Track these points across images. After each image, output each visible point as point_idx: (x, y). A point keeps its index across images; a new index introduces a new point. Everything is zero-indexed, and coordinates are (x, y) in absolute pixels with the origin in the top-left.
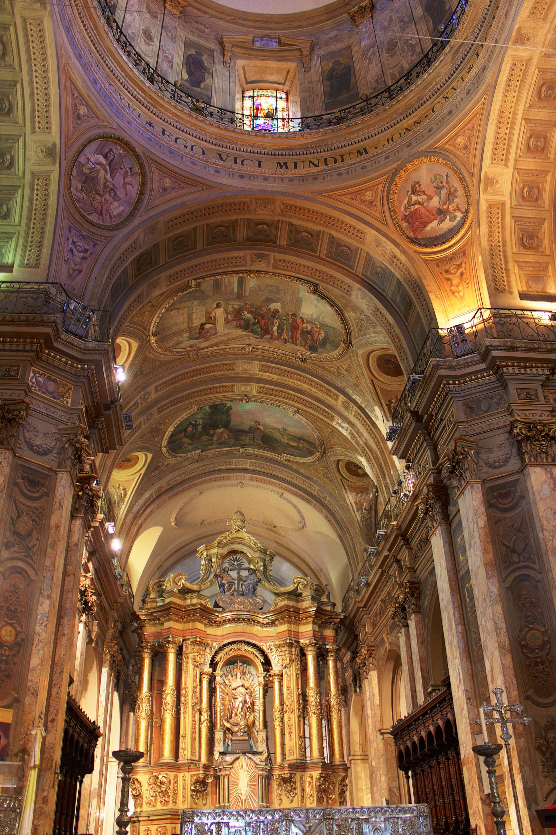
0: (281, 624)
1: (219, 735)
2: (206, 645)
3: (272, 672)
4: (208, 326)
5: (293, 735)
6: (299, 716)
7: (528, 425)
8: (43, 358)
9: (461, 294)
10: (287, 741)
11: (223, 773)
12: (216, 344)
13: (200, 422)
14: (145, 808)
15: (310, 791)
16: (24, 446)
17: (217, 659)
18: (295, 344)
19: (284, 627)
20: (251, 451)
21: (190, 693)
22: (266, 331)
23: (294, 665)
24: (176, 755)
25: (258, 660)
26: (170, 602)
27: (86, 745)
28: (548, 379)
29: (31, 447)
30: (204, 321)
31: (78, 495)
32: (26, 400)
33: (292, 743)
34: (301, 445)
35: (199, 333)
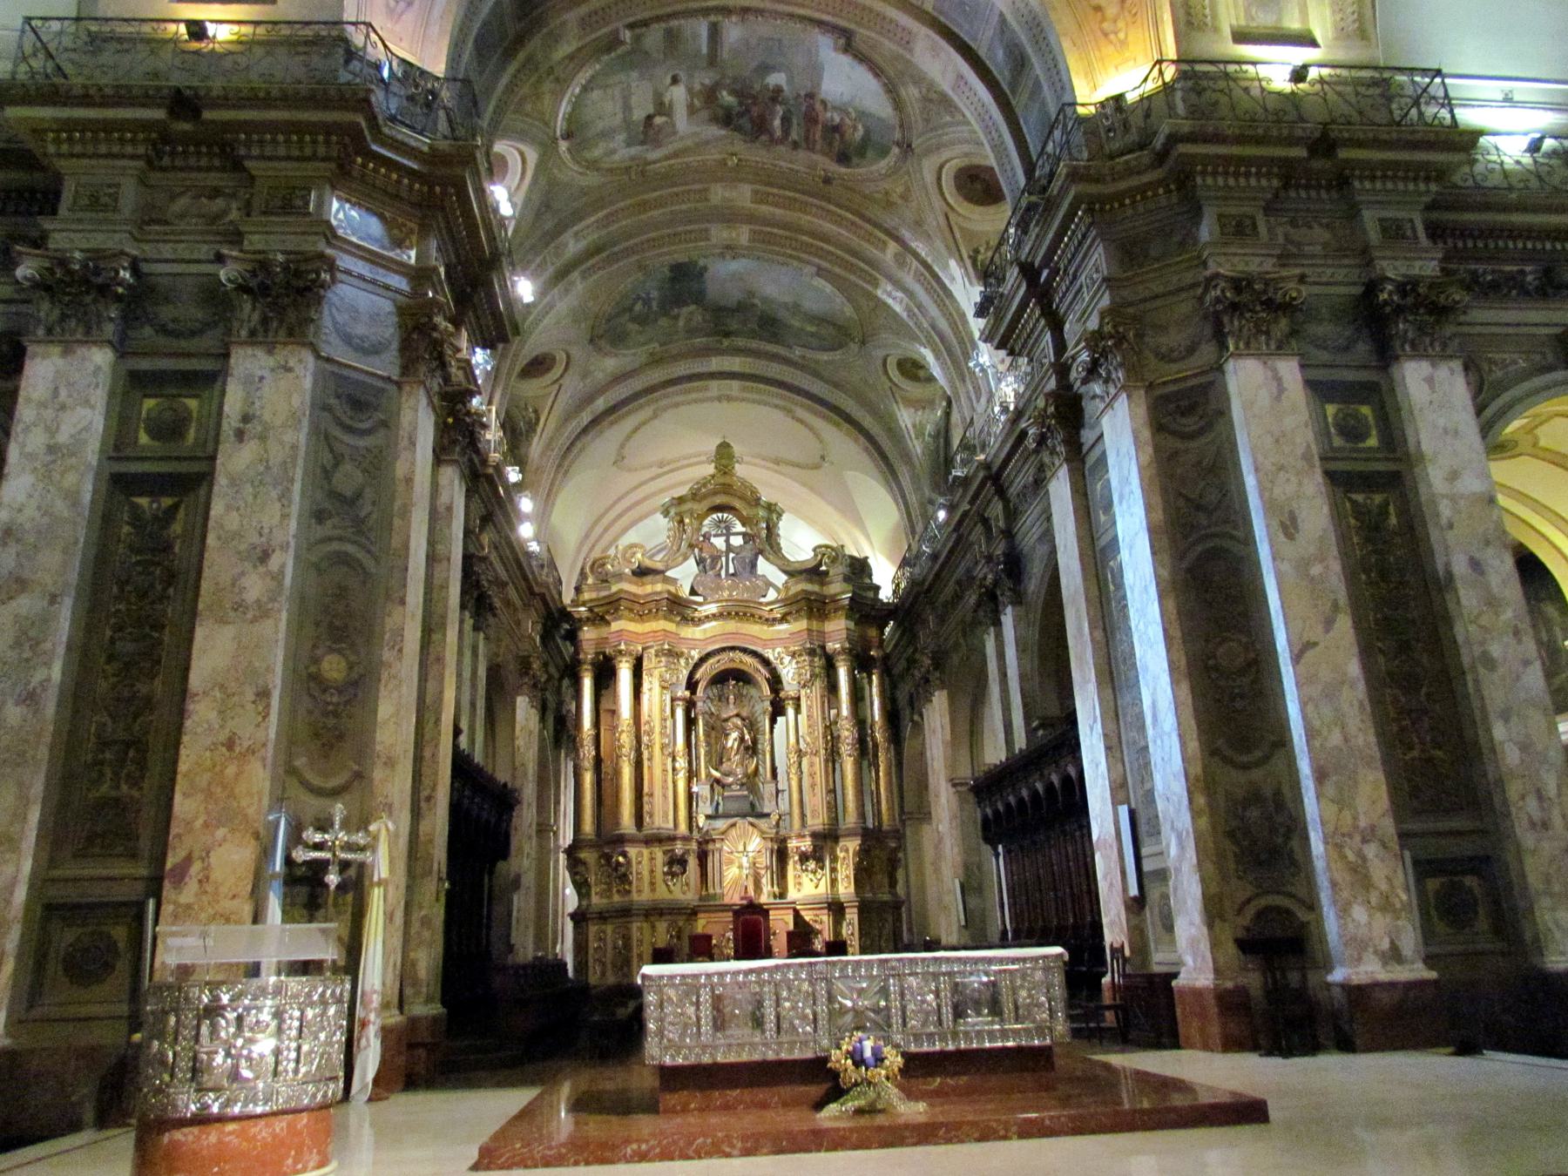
0: (796, 620)
2: (679, 655)
3: (782, 694)
4: (658, 120)
5: (818, 789)
6: (826, 761)
7: (1238, 284)
8: (355, 173)
9: (1121, 35)
10: (806, 798)
11: (710, 847)
12: (675, 155)
13: (655, 294)
14: (595, 899)
15: (846, 872)
16: (334, 339)
17: (698, 676)
18: (812, 150)
19: (803, 624)
20: (740, 342)
21: (657, 730)
22: (759, 128)
23: (818, 683)
25: (761, 675)
26: (621, 591)
27: (493, 820)
28: (1276, 196)
29: (348, 339)
30: (651, 110)
31: (445, 423)
32: (329, 251)
34: (823, 332)
35: (645, 133)
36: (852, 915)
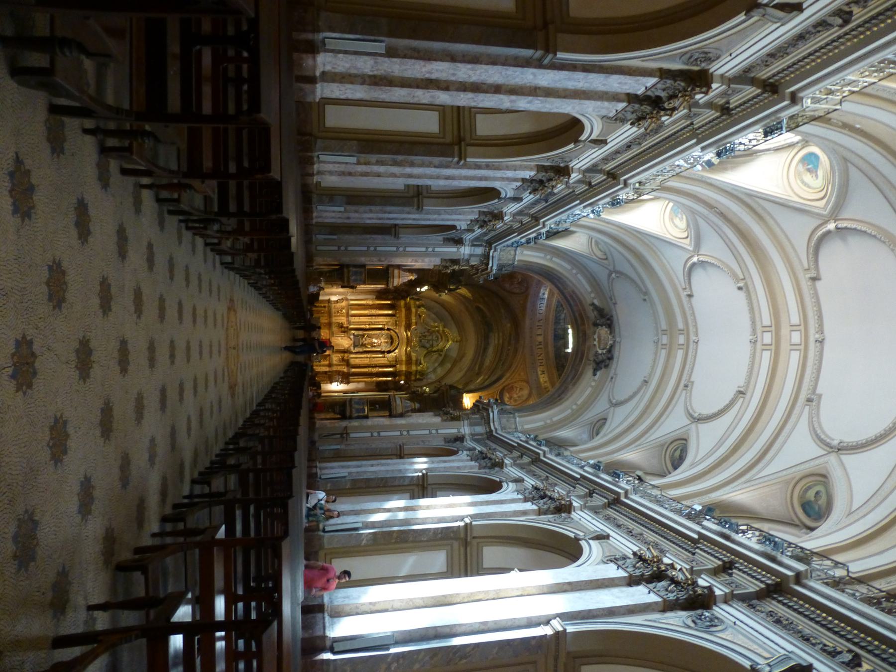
1: (361, 333)
15: (339, 368)
19: (404, 358)
33: (357, 361)
36: (327, 369)
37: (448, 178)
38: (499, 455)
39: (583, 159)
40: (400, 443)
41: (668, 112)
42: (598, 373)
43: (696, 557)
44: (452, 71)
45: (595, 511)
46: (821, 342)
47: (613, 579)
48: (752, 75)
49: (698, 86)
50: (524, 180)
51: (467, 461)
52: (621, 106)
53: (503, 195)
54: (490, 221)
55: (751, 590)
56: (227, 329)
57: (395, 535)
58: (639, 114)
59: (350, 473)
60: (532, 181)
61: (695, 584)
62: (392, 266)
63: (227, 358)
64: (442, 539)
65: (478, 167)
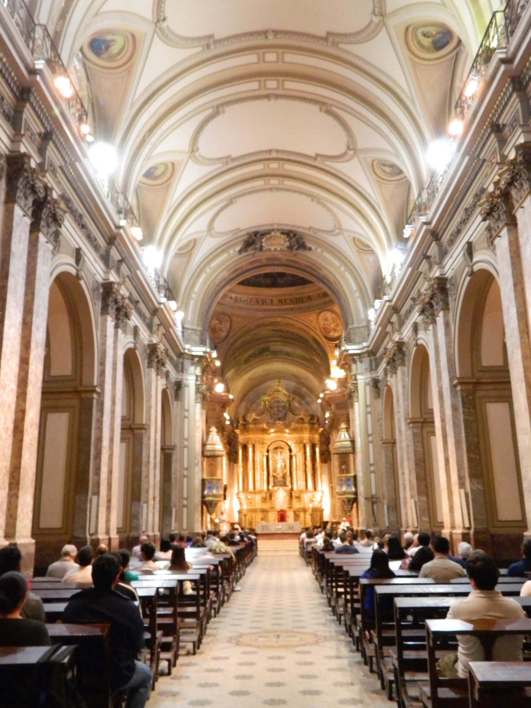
1: (271, 479)
24: (254, 488)
25: (287, 449)
37: (114, 403)
38: (390, 345)
39: (95, 269)
40: (380, 443)
41: (49, 193)
42: (308, 245)
43: (487, 157)
44: (6, 409)
45: (443, 253)
46: (276, 32)
47: (510, 243)
48: (12, 112)
49: (23, 165)
50: (116, 327)
51: (396, 377)
52: (42, 238)
53: (132, 346)
54: (158, 357)
55: (519, 106)
56: (258, 647)
57: (472, 456)
58: (50, 220)
59: (412, 497)
60: (117, 318)
61: (513, 162)
62: (203, 452)
63: (287, 647)
64: (474, 408)
65: (102, 373)
